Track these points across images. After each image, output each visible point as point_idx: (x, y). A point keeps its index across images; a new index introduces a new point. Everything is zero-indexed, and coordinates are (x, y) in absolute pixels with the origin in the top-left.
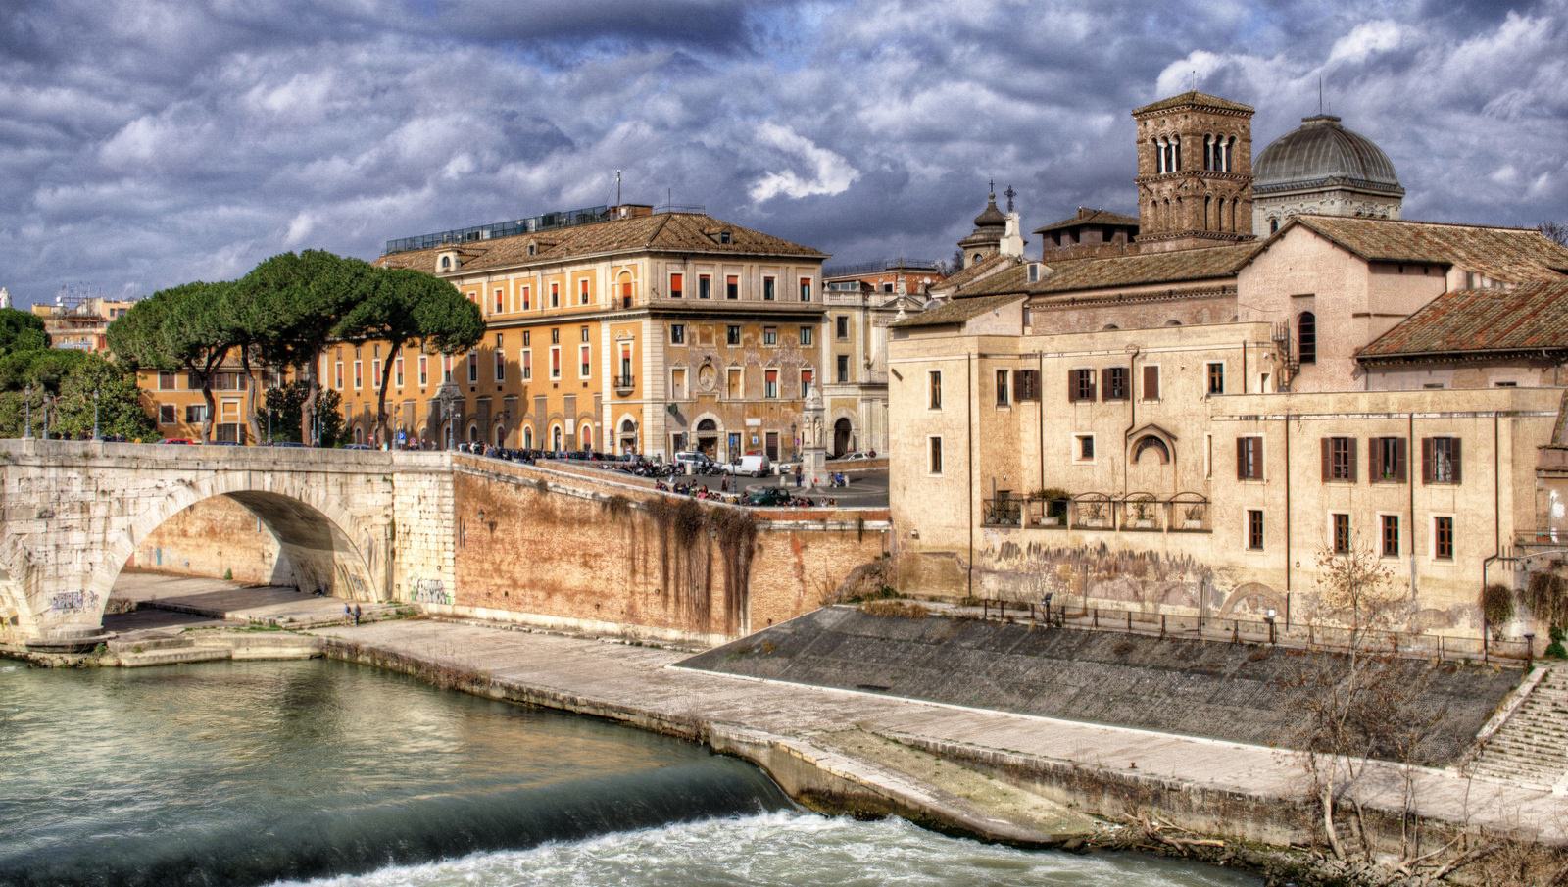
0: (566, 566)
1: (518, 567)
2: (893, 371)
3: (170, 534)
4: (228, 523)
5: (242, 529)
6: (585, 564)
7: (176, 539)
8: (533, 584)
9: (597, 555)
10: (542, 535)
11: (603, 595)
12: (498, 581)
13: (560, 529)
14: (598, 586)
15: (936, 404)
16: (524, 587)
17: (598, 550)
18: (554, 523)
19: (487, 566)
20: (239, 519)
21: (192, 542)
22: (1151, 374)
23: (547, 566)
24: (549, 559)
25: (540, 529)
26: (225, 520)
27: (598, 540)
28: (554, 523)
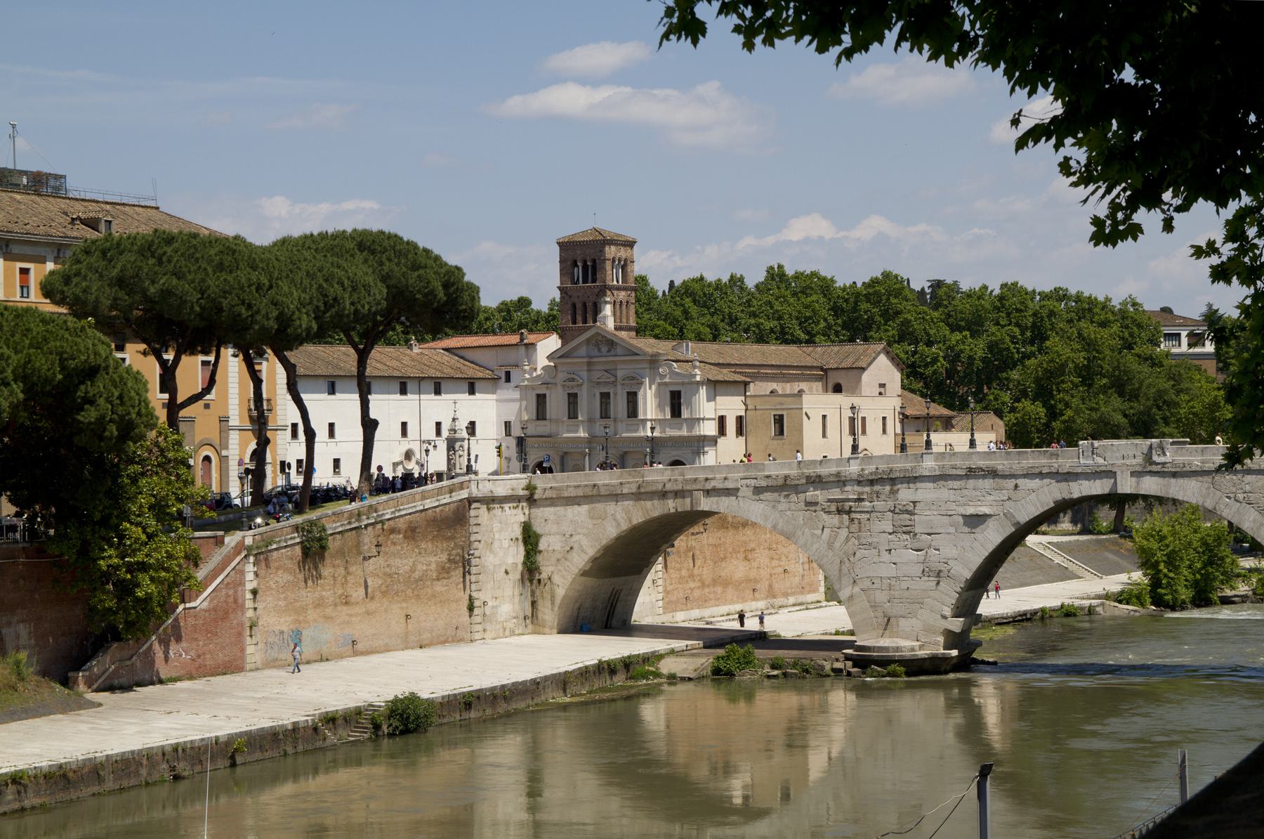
0: (735, 563)
1: (705, 569)
2: (806, 414)
3: (317, 606)
4: (417, 575)
5: (438, 580)
6: (746, 558)
7: (329, 611)
8: (714, 582)
9: (753, 550)
10: (720, 539)
11: (756, 581)
12: (692, 585)
13: (731, 532)
14: (753, 574)
15: (824, 436)
16: (708, 586)
17: (753, 545)
18: (727, 528)
19: (684, 573)
20: (433, 566)
21: (359, 609)
22: (864, 419)
23: (724, 564)
24: (725, 558)
25: (719, 534)
26: (413, 570)
27: (753, 538)
28: (727, 528)
